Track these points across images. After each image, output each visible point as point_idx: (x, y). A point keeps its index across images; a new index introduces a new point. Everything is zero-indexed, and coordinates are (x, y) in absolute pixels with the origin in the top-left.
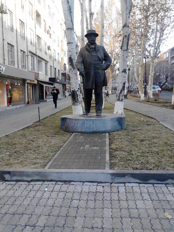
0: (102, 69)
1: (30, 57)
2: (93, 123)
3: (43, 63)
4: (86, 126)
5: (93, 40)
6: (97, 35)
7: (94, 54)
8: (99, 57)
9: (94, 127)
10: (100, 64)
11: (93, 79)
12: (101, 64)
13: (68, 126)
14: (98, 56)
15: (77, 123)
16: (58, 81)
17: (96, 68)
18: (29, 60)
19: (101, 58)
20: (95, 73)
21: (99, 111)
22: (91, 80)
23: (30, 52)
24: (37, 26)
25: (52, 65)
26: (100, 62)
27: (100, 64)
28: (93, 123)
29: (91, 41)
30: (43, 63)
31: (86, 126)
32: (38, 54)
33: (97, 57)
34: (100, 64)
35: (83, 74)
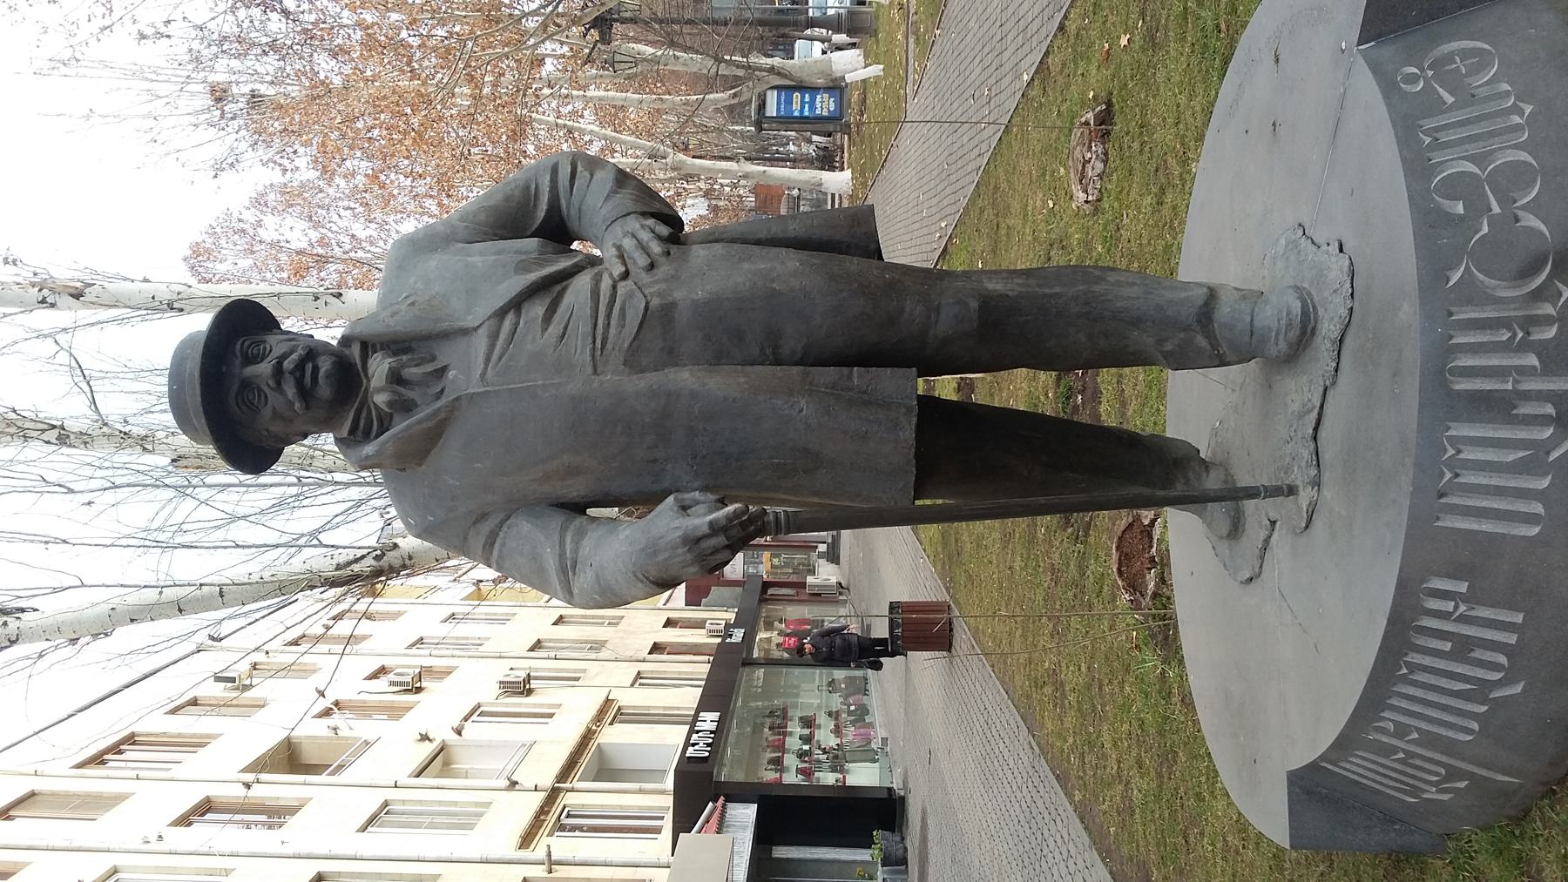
0: (664, 269)
1: (564, 846)
3: (613, 736)
4: (1530, 519)
5: (300, 365)
6: (243, 323)
7: (467, 368)
8: (517, 304)
12: (597, 281)
13: (1462, 775)
14: (501, 314)
15: (1463, 648)
16: (738, 635)
17: (659, 336)
18: (581, 855)
19: (533, 277)
21: (1224, 311)
23: (527, 840)
24: (357, 771)
25: (633, 669)
26: (583, 281)
29: (305, 394)
30: (613, 736)
31: (1530, 519)
32: (548, 780)
35: (715, 529)
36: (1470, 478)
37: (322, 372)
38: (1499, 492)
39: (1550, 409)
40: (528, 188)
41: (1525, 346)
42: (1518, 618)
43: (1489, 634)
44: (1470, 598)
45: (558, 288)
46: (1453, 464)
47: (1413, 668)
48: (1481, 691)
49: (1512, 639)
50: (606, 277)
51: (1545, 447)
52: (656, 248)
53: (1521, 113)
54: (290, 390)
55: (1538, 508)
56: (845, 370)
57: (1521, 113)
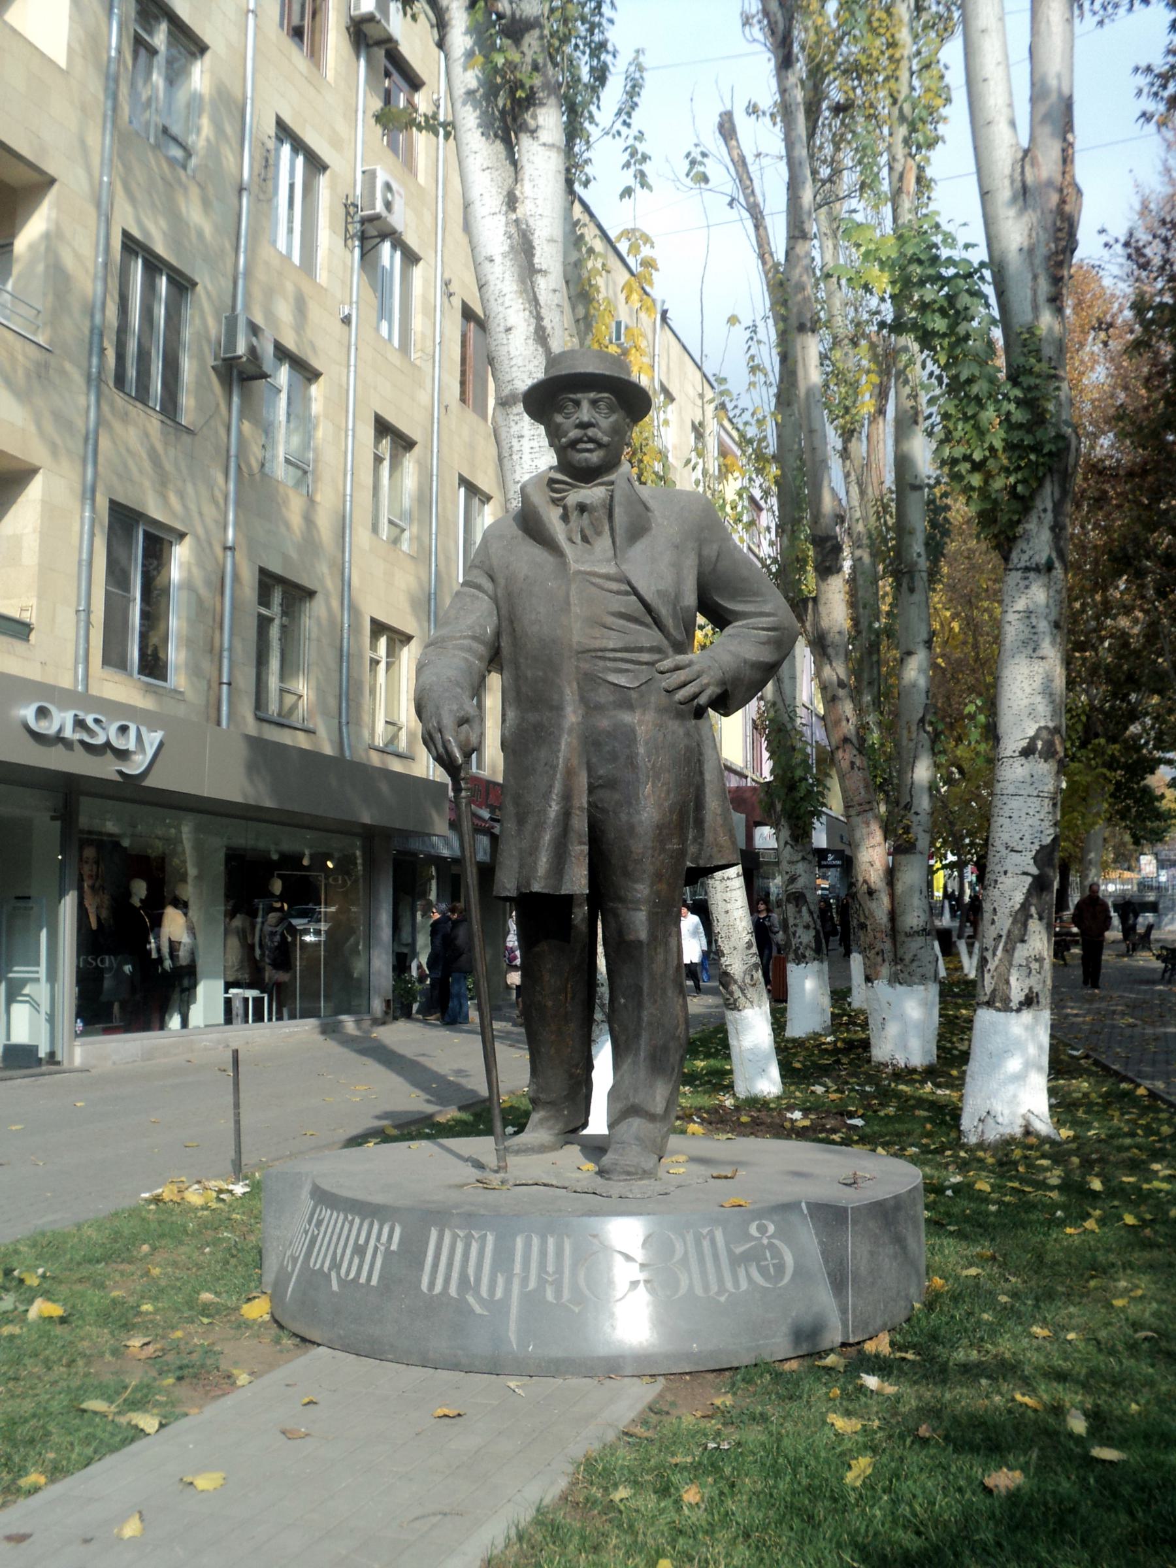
2: (503, 1259)
4: (432, 1284)
8: (635, 592)
9: (499, 1308)
10: (640, 650)
11: (567, 797)
15: (360, 1251)
20: (592, 742)
22: (554, 809)
27: (645, 657)
28: (503, 1259)
31: (432, 1284)
33: (614, 586)
34: (640, 650)
36: (460, 1246)
37: (587, 455)
38: (450, 1265)
39: (499, 1294)
40: (756, 594)
41: (542, 1282)
42: (374, 1282)
43: (366, 1267)
44: (388, 1253)
45: (649, 620)
46: (469, 1237)
47: (352, 1223)
48: (336, 1265)
49: (363, 1280)
50: (656, 657)
51: (477, 1290)
52: (681, 695)
53: (719, 1293)
54: (574, 434)
55: (438, 1288)
56: (586, 839)
57: (719, 1293)
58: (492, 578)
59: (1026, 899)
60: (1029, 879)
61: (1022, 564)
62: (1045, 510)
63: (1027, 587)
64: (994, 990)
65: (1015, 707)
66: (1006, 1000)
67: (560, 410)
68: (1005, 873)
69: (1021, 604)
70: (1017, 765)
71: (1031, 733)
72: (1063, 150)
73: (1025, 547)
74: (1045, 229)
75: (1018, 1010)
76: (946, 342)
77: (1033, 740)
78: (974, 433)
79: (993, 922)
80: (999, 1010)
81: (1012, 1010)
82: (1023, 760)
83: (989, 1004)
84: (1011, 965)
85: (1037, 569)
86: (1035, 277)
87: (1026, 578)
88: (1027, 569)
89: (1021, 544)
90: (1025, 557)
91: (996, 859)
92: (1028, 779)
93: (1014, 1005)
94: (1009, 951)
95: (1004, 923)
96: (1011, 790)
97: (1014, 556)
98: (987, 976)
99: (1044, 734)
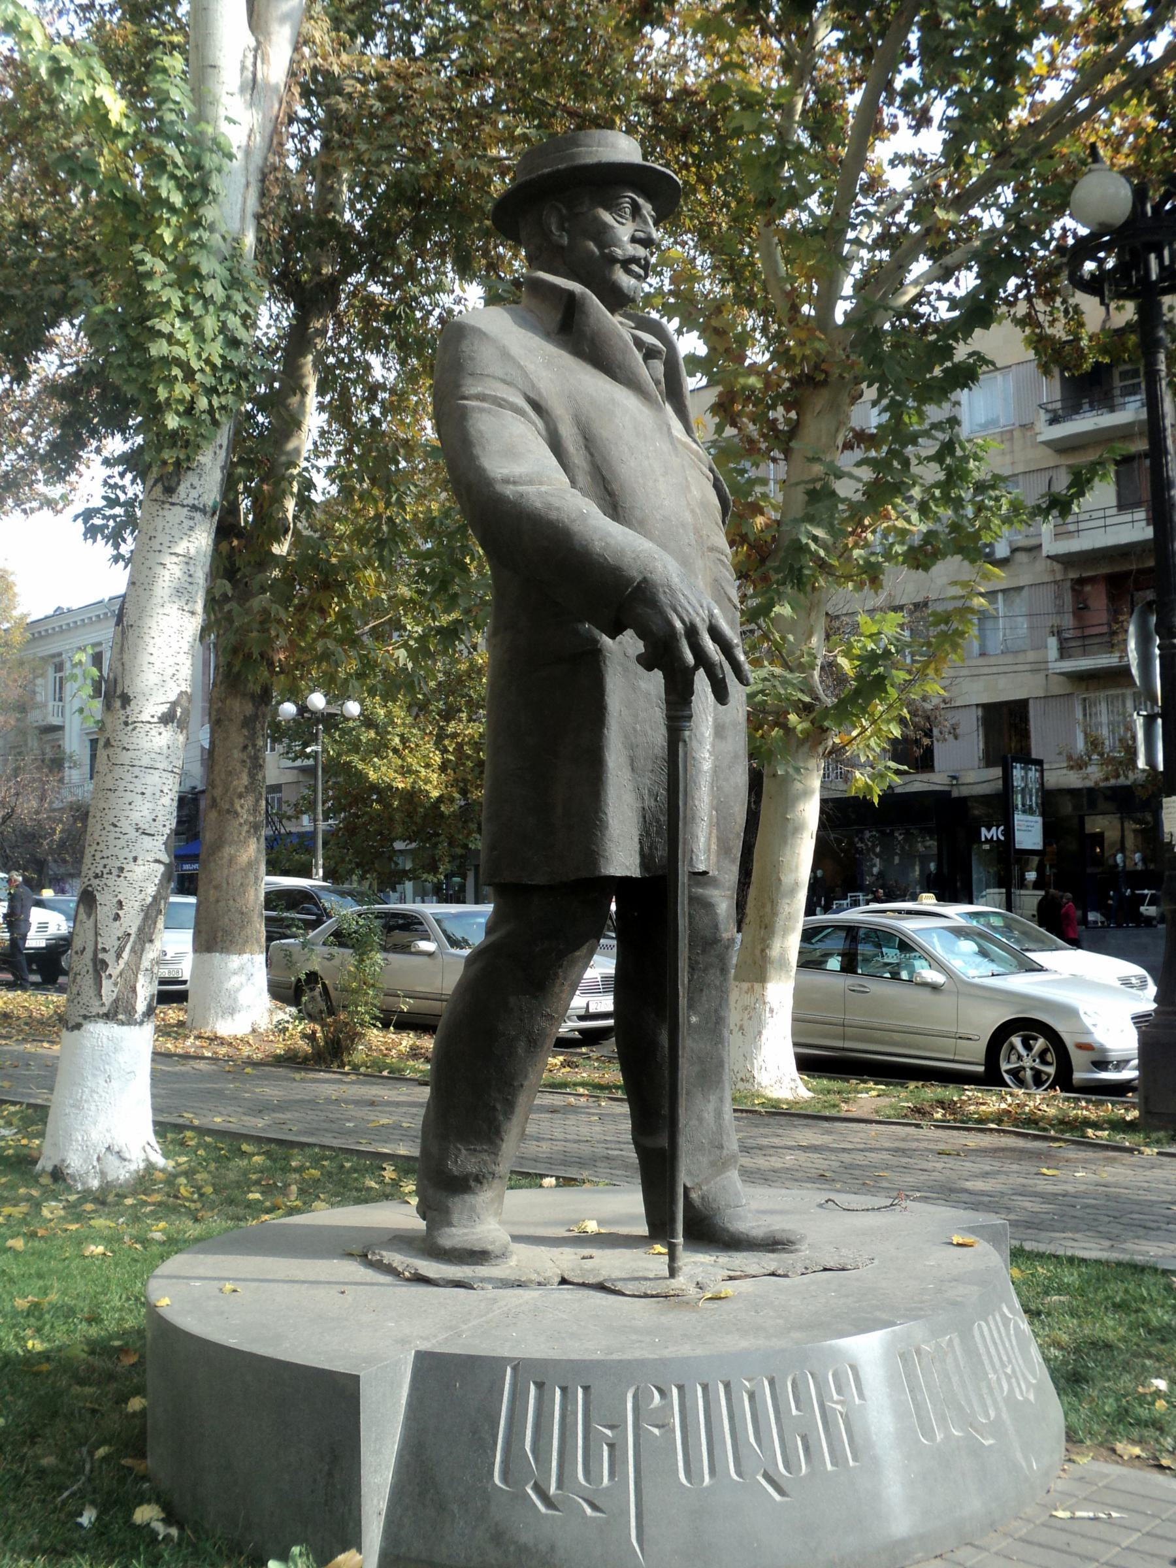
58: (537, 407)
59: (158, 891)
60: (161, 868)
61: (190, 501)
62: (221, 446)
63: (191, 529)
64: (116, 1001)
65: (158, 665)
66: (130, 1011)
67: (612, 206)
68: (135, 859)
69: (180, 548)
70: (154, 732)
71: (173, 698)
72: (292, 61)
73: (196, 482)
74: (263, 137)
75: (141, 1023)
76: (174, 220)
77: (174, 704)
78: (192, 338)
79: (117, 917)
80: (123, 1023)
81: (135, 1023)
82: (162, 729)
83: (109, 1017)
84: (138, 969)
85: (203, 511)
86: (248, 185)
87: (192, 518)
88: (194, 508)
89: (191, 478)
90: (194, 493)
91: (122, 843)
92: (165, 751)
93: (138, 1016)
94: (138, 952)
95: (131, 920)
96: (145, 761)
97: (182, 489)
98: (106, 985)
99: (184, 702)
